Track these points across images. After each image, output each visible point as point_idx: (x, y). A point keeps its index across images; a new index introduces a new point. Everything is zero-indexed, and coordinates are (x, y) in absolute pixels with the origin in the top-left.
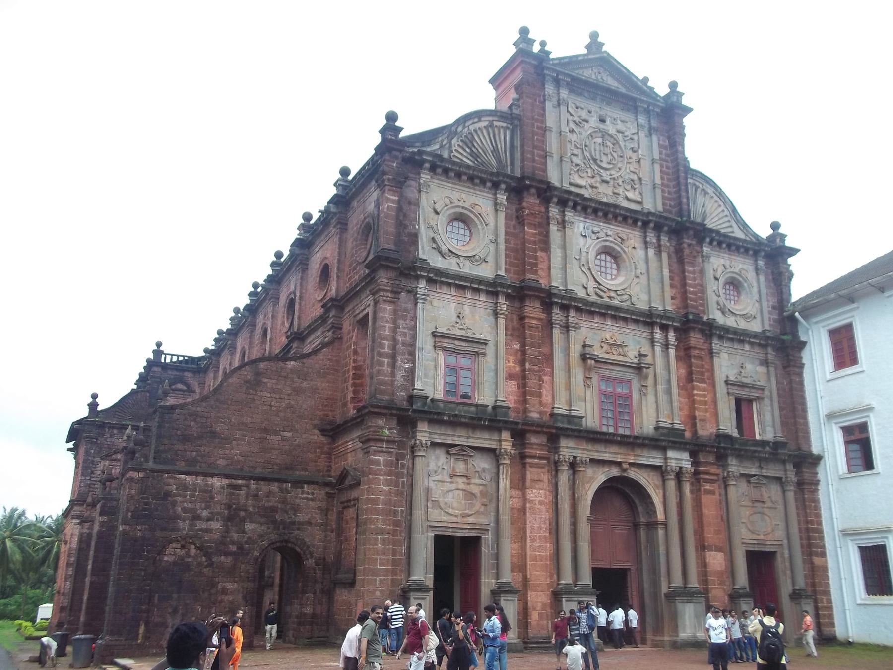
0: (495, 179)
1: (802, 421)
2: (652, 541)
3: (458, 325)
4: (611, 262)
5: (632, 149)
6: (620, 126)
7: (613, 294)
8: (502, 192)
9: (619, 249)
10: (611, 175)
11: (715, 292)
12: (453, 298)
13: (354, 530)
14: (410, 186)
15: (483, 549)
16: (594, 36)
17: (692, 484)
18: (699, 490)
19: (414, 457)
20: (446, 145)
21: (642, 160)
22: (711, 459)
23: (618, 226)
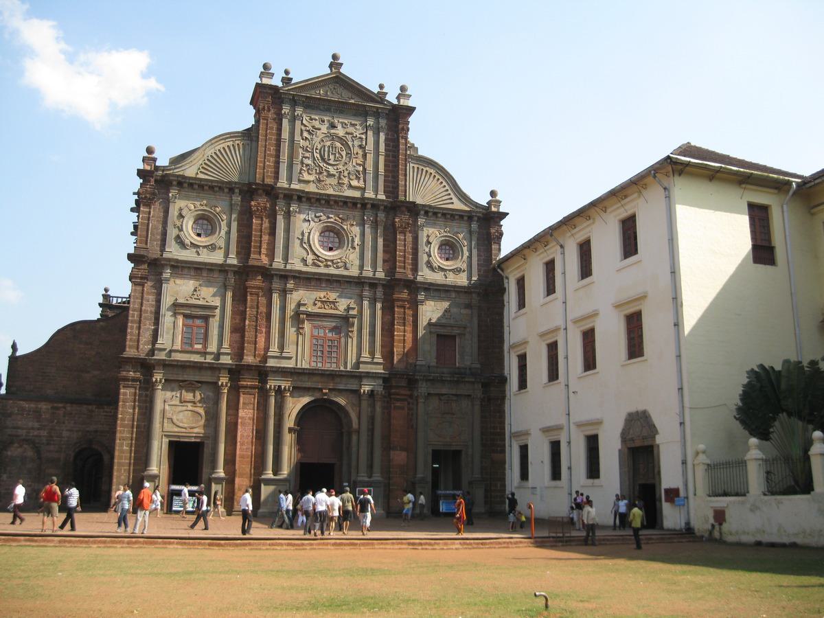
3: (196, 297)
6: (351, 129)
7: (329, 263)
15: (205, 450)
16: (335, 57)
18: (391, 406)
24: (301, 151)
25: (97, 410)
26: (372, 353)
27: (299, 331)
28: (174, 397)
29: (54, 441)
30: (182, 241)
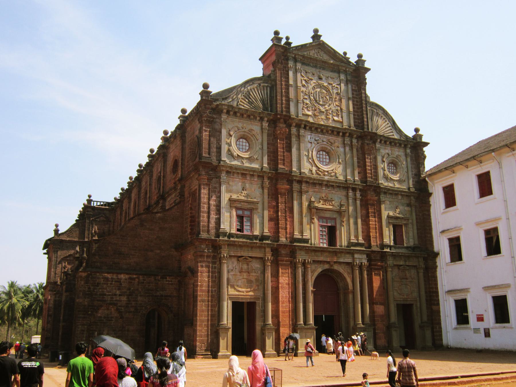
1: (429, 235)
2: (346, 301)
4: (326, 155)
5: (337, 93)
7: (326, 173)
9: (330, 148)
10: (325, 108)
11: (383, 167)
12: (240, 180)
13: (192, 299)
14: (217, 122)
15: (257, 307)
16: (316, 31)
17: (367, 271)
19: (220, 263)
20: (235, 98)
23: (329, 136)
24: (302, 94)
25: (161, 279)
26: (357, 237)
27: (311, 221)
28: (234, 268)
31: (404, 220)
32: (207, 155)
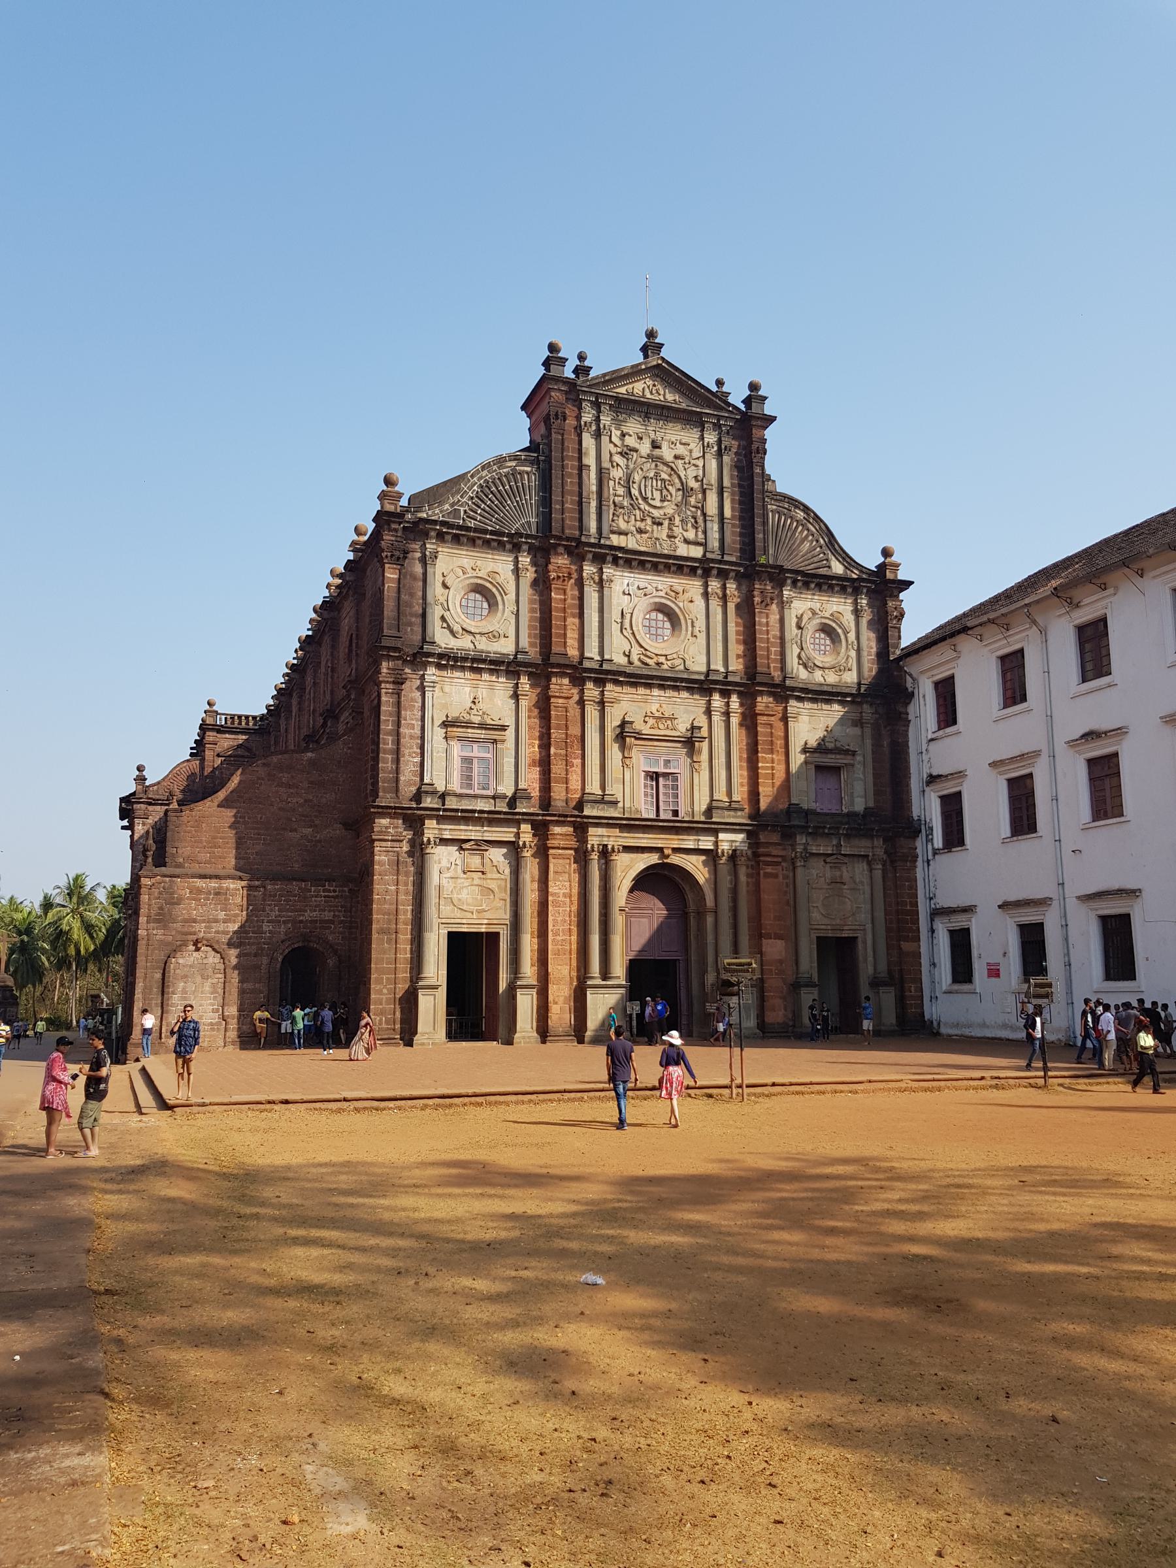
0: (515, 541)
4: (663, 621)
5: (696, 477)
6: (681, 450)
7: (662, 659)
8: (525, 554)
16: (651, 334)
18: (759, 874)
21: (708, 491)
22: (775, 838)
29: (250, 938)
30: (448, 625)
31: (842, 756)
32: (393, 632)
